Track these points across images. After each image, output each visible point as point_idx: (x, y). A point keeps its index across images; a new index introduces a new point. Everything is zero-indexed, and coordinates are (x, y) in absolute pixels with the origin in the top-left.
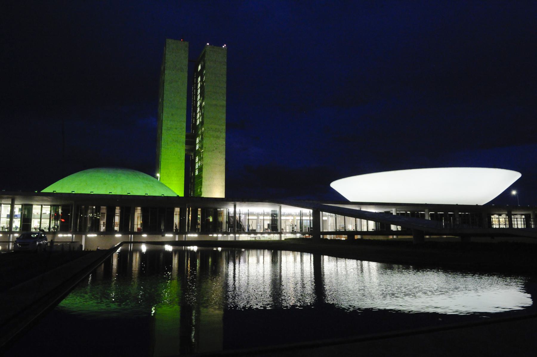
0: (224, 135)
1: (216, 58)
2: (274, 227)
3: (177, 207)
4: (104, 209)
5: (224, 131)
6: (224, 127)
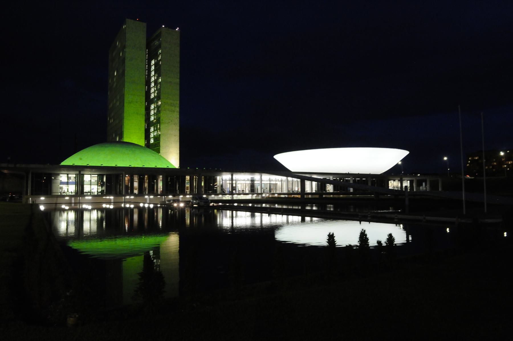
0: (178, 109)
2: (253, 189)
3: (188, 175)
4: (136, 179)
5: (178, 105)
6: (178, 102)
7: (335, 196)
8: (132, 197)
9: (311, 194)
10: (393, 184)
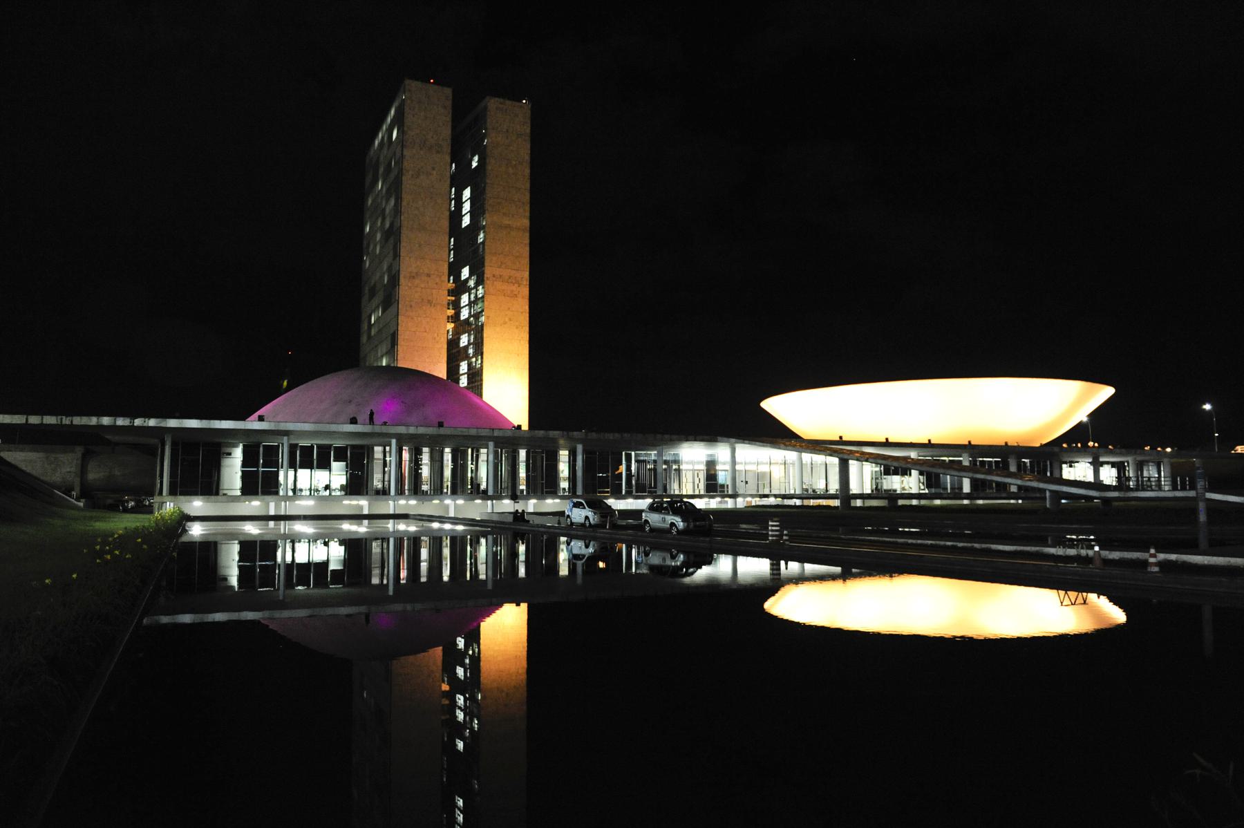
0: (525, 291)
1: (509, 127)
5: (526, 282)
6: (527, 274)
7: (923, 502)
8: (413, 502)
9: (862, 496)
10: (1080, 471)
